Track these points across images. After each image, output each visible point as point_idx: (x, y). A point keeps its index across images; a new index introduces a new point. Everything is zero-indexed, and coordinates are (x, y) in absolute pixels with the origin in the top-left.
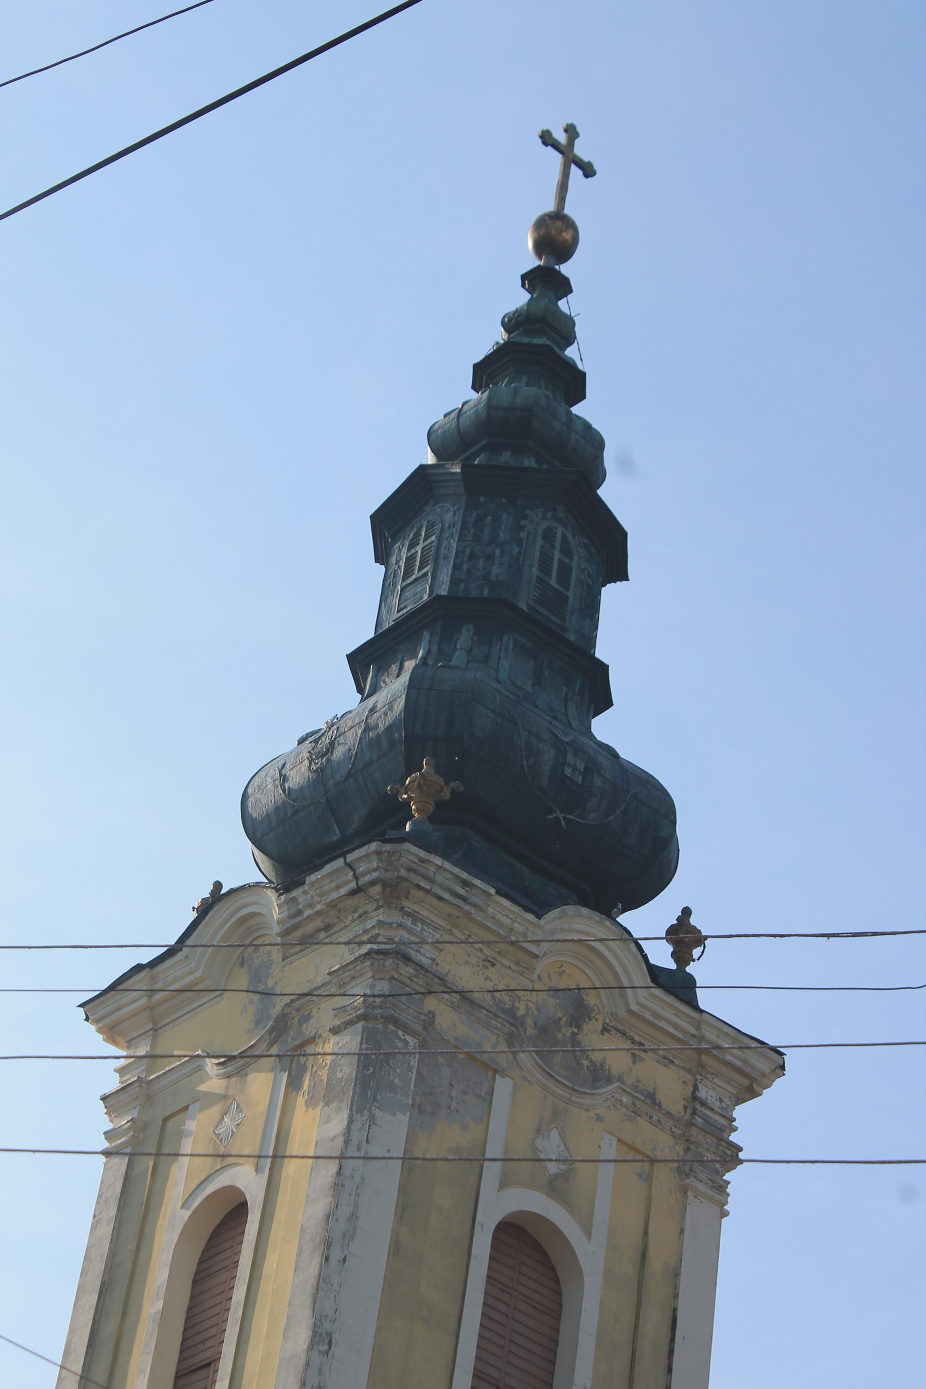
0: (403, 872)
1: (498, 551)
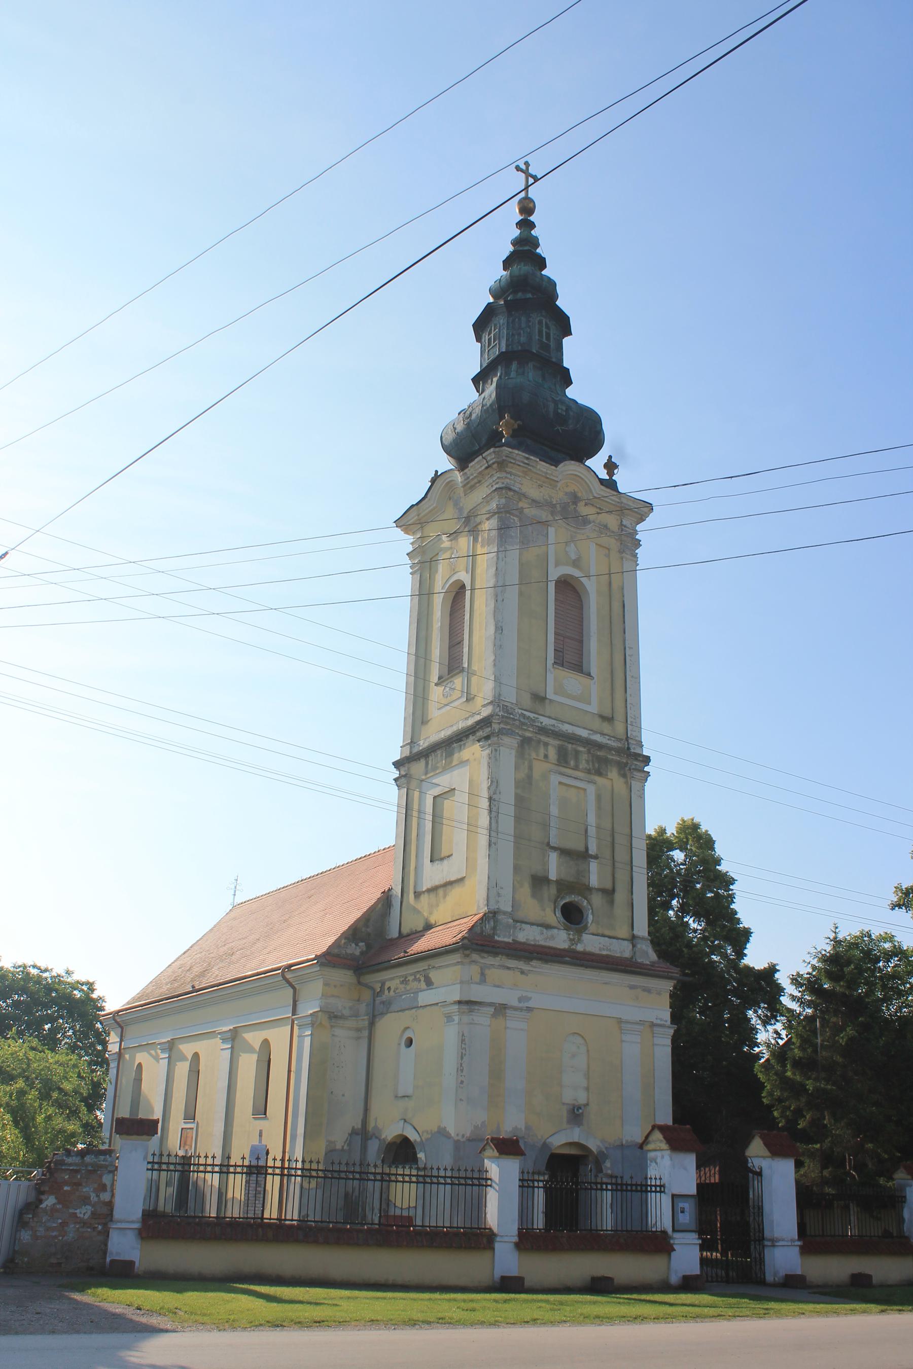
0: (504, 458)
1: (522, 332)
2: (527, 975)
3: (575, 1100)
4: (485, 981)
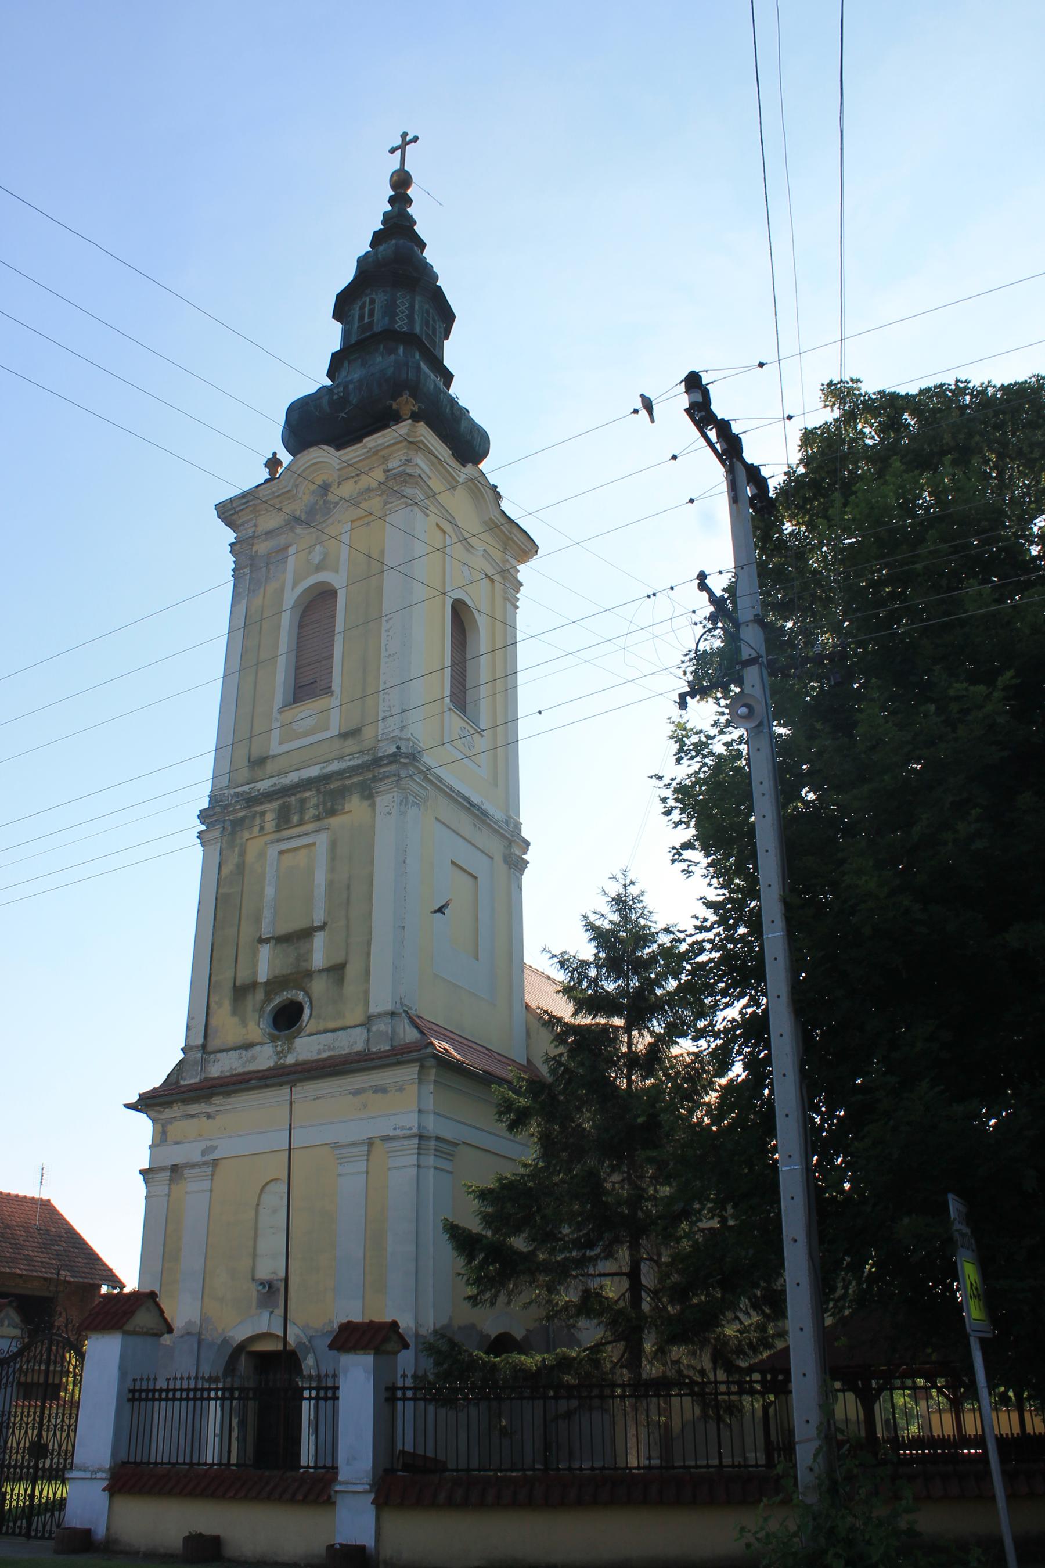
2: (214, 1118)
3: (274, 1273)
4: (166, 1141)
